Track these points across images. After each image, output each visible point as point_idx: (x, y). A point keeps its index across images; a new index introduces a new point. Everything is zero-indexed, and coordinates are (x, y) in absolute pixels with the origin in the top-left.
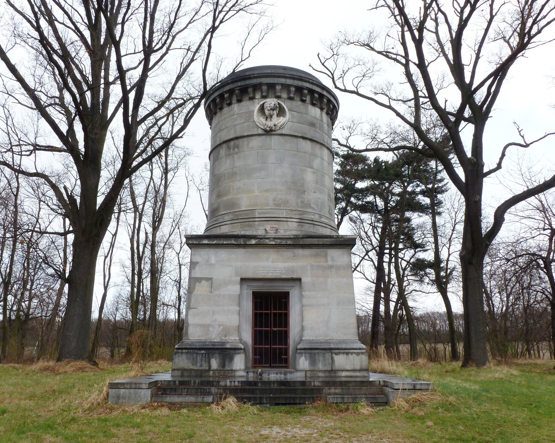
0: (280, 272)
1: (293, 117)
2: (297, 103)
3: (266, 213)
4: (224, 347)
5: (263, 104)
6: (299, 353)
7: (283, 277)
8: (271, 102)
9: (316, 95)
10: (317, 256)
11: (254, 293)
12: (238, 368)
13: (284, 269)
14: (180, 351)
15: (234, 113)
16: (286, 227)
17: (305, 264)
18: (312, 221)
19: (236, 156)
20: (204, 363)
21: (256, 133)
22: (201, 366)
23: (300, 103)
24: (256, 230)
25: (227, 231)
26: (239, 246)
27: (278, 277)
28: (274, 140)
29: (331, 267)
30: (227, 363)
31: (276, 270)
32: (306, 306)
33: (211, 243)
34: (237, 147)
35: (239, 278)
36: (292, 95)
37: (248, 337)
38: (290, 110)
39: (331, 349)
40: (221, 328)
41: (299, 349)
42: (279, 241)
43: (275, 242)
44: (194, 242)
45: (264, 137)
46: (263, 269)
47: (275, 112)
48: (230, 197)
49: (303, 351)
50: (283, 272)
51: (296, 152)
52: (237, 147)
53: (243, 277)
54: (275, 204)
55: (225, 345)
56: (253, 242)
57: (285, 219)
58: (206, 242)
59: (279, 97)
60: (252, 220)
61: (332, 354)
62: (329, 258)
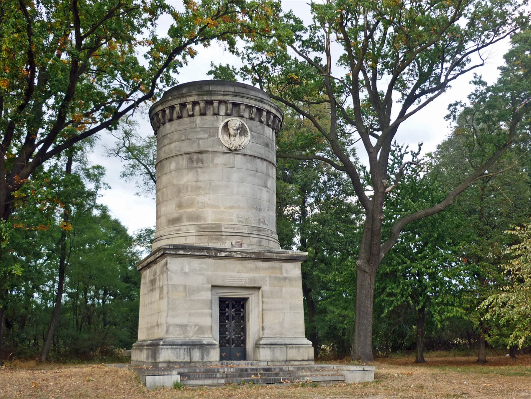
1: (253, 137)
2: (256, 123)
3: (232, 228)
5: (227, 123)
7: (247, 285)
8: (235, 122)
9: (272, 117)
10: (273, 268)
11: (220, 298)
12: (214, 360)
14: (165, 347)
15: (196, 126)
16: (249, 242)
18: (267, 236)
19: (199, 170)
20: (186, 356)
21: (220, 150)
22: (184, 359)
23: (259, 123)
24: (224, 243)
25: (194, 241)
26: (210, 257)
28: (238, 159)
29: (285, 278)
30: (205, 356)
33: (187, 253)
34: (202, 161)
35: (210, 286)
36: (253, 116)
38: (251, 130)
39: (286, 344)
40: (197, 327)
42: (244, 254)
44: (172, 252)
45: (228, 155)
47: (239, 132)
48: (194, 209)
49: (265, 346)
51: (254, 172)
52: (202, 161)
54: (238, 220)
56: (223, 254)
57: (248, 235)
58: (181, 252)
59: (241, 117)
60: (219, 234)
61: (287, 347)
62: (284, 271)
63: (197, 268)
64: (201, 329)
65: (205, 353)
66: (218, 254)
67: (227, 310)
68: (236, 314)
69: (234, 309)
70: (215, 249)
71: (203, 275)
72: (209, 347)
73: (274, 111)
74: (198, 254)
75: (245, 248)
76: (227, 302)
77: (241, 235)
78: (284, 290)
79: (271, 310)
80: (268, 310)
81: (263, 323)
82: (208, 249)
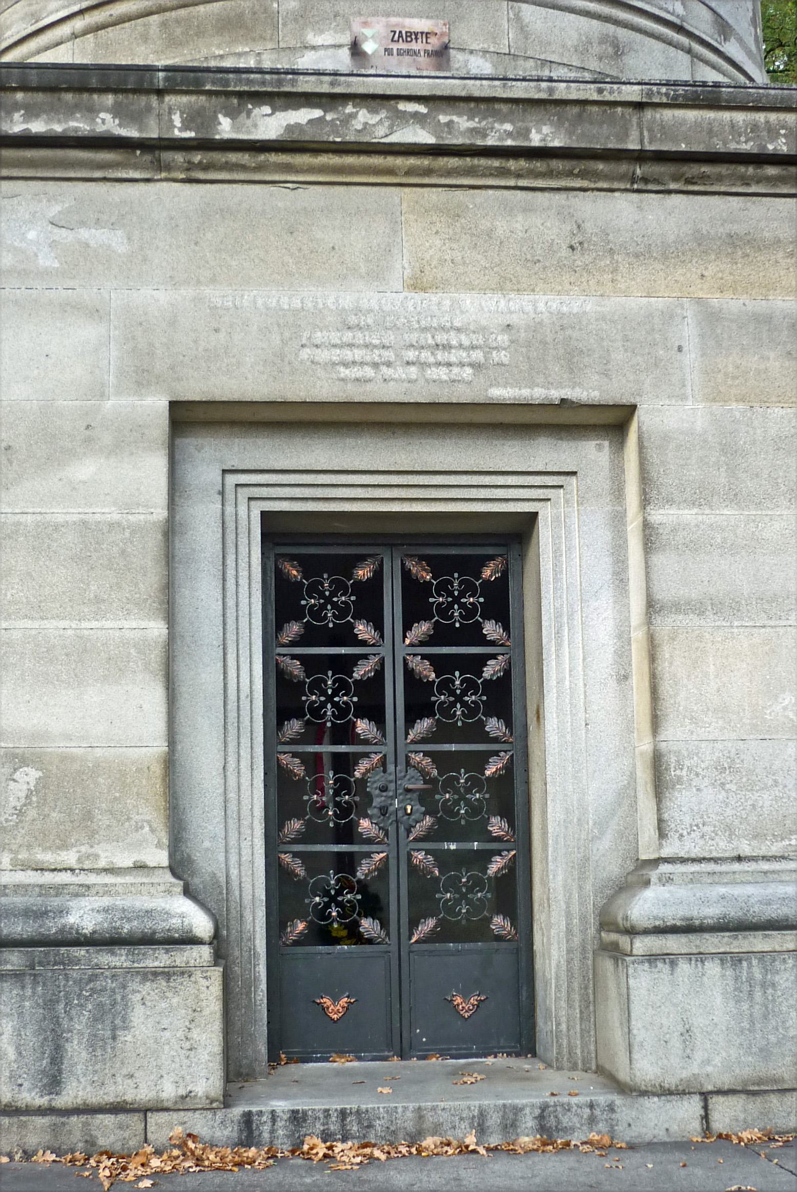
0: (477, 356)
4: (51, 927)
6: (652, 958)
7: (501, 393)
12: (169, 1091)
13: (503, 339)
17: (658, 303)
27: (463, 395)
31: (447, 347)
32: (677, 607)
35: (167, 403)
40: (29, 776)
41: (646, 932)
42: (463, 123)
43: (437, 128)
46: (348, 336)
49: (673, 943)
50: (503, 357)
53: (193, 391)
55: (62, 911)
63: (47, 260)
65: (80, 1023)
66: (226, 129)
67: (363, 630)
68: (440, 664)
69: (422, 628)
71: (96, 313)
72: (119, 959)
74: (38, 127)
76: (363, 573)
80: (697, 608)
81: (656, 723)
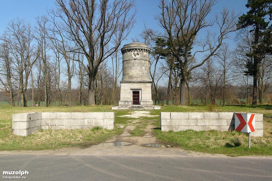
26: (130, 83)
29: (147, 87)
37: (132, 99)
58: (124, 82)
59: (137, 51)
64: (128, 98)
70: (131, 81)
73: (146, 49)
75: (138, 80)
77: (137, 78)
78: (147, 89)
79: (144, 94)
82: (129, 81)
